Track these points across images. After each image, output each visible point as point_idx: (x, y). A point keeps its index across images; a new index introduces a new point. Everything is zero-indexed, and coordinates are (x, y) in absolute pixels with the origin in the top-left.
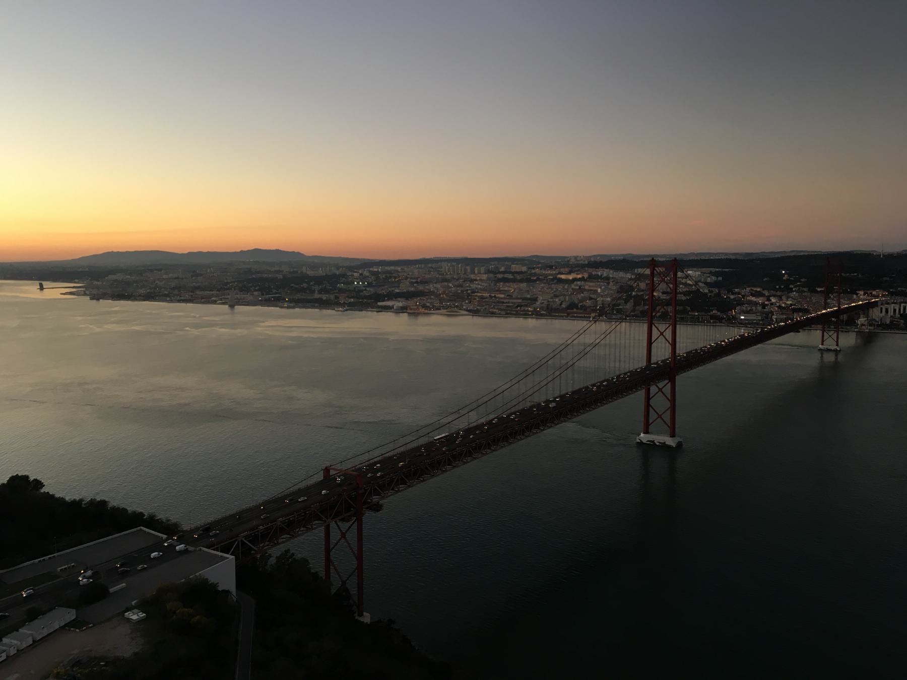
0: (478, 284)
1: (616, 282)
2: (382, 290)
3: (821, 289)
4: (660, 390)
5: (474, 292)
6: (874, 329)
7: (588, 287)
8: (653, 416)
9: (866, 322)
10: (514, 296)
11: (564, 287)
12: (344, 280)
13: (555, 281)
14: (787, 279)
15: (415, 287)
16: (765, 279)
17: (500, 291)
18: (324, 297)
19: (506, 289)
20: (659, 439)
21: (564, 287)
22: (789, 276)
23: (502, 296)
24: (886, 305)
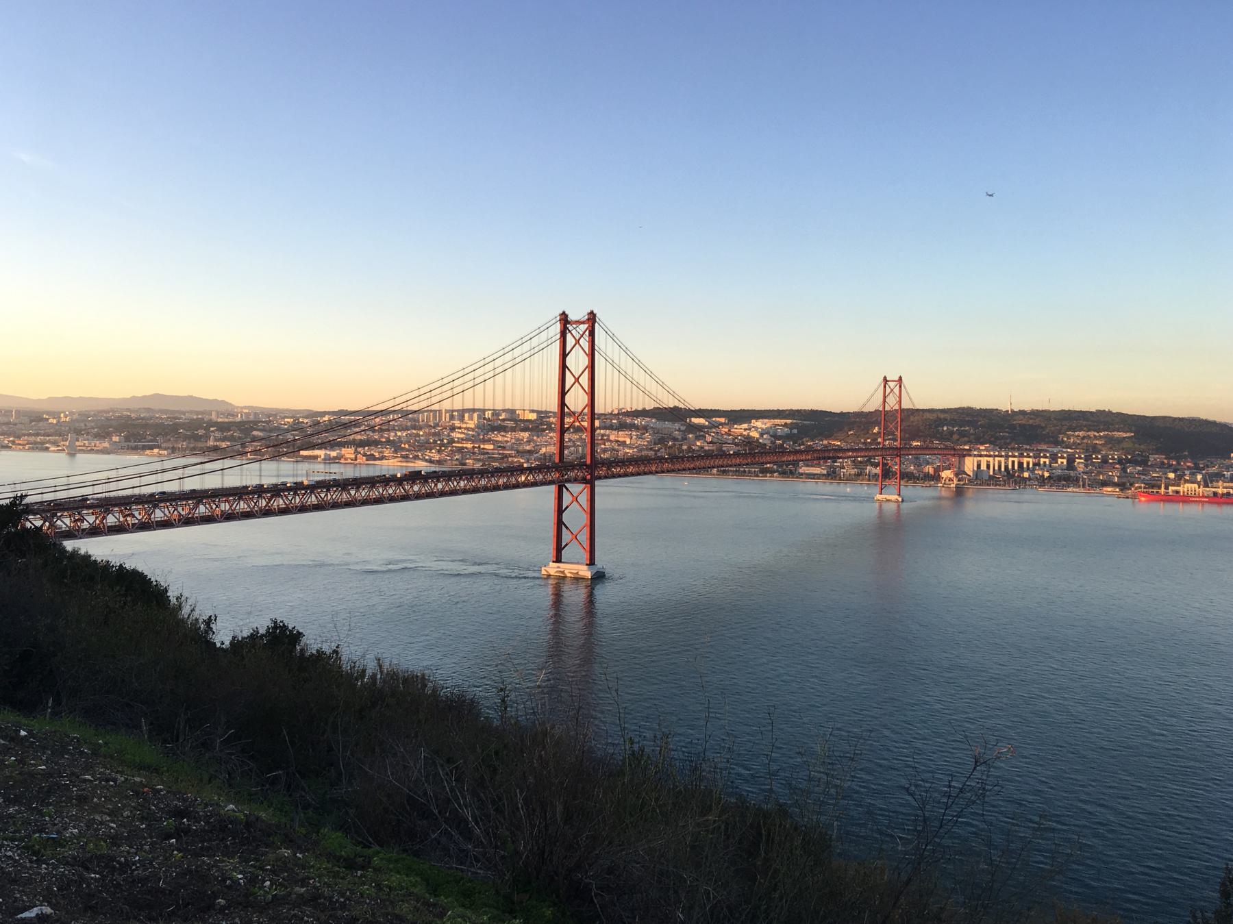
0: (462, 433)
1: (656, 431)
2: (319, 438)
3: (916, 444)
5: (452, 441)
7: (614, 436)
8: (566, 536)
10: (507, 448)
11: (580, 437)
12: (264, 426)
13: (572, 430)
15: (368, 435)
17: (489, 441)
18: (224, 445)
19: (500, 438)
20: (569, 569)
21: (581, 437)
23: (491, 447)
24: (988, 459)
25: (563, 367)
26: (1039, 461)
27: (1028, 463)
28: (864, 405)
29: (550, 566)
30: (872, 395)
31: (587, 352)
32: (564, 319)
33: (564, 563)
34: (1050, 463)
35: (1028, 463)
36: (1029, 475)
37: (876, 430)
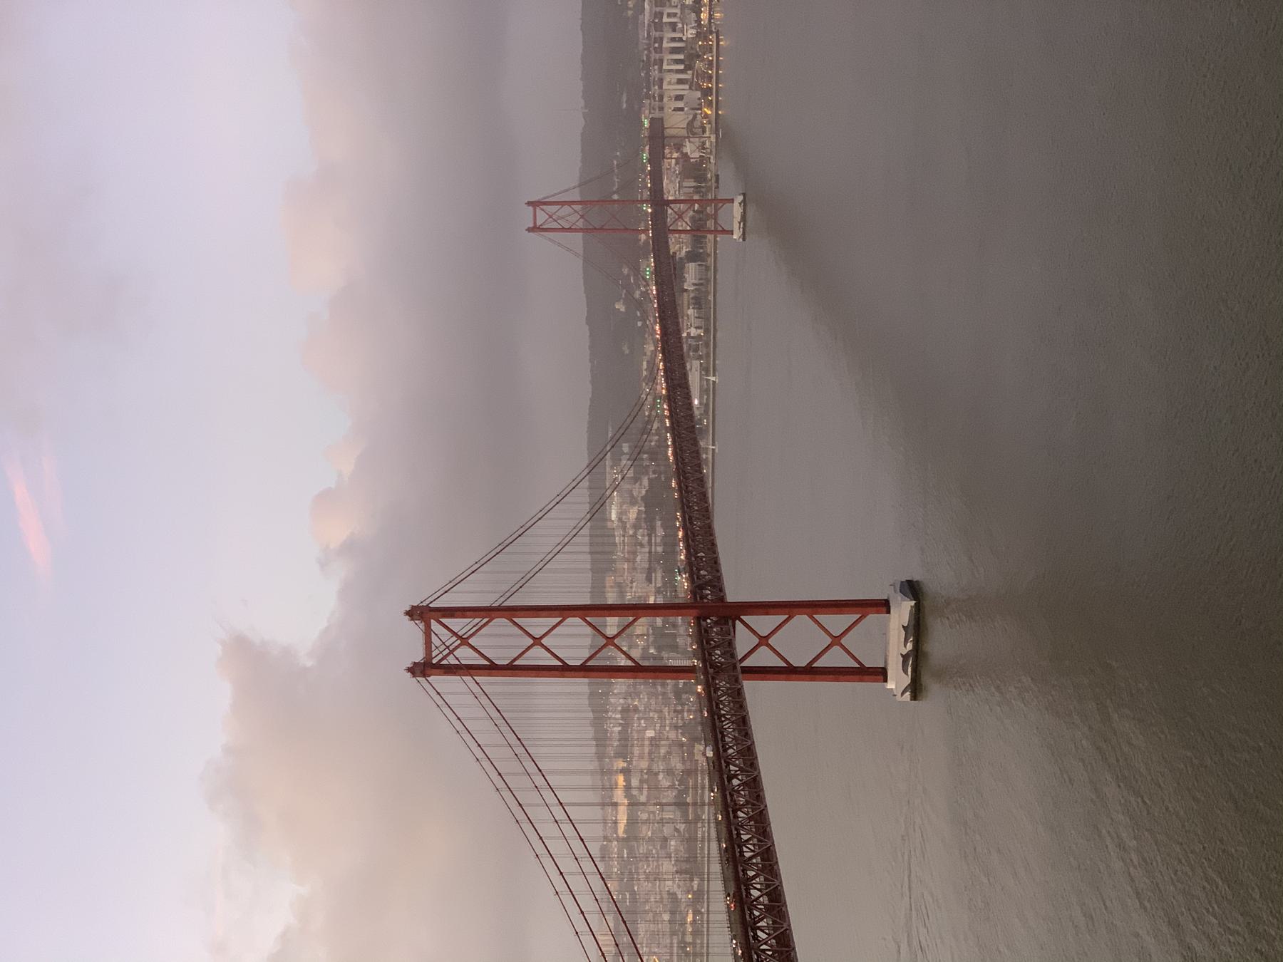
4: (764, 641)
6: (710, 123)
8: (835, 659)
9: (691, 139)
11: (647, 822)
14: (623, 304)
16: (627, 352)
20: (897, 646)
21: (647, 822)
22: (618, 301)
24: (665, 100)
25: (512, 669)
26: (666, 23)
27: (673, 40)
28: (576, 254)
29: (893, 687)
30: (559, 244)
31: (486, 620)
32: (422, 669)
33: (886, 662)
34: (671, 6)
35: (673, 40)
36: (693, 28)
37: (620, 306)
